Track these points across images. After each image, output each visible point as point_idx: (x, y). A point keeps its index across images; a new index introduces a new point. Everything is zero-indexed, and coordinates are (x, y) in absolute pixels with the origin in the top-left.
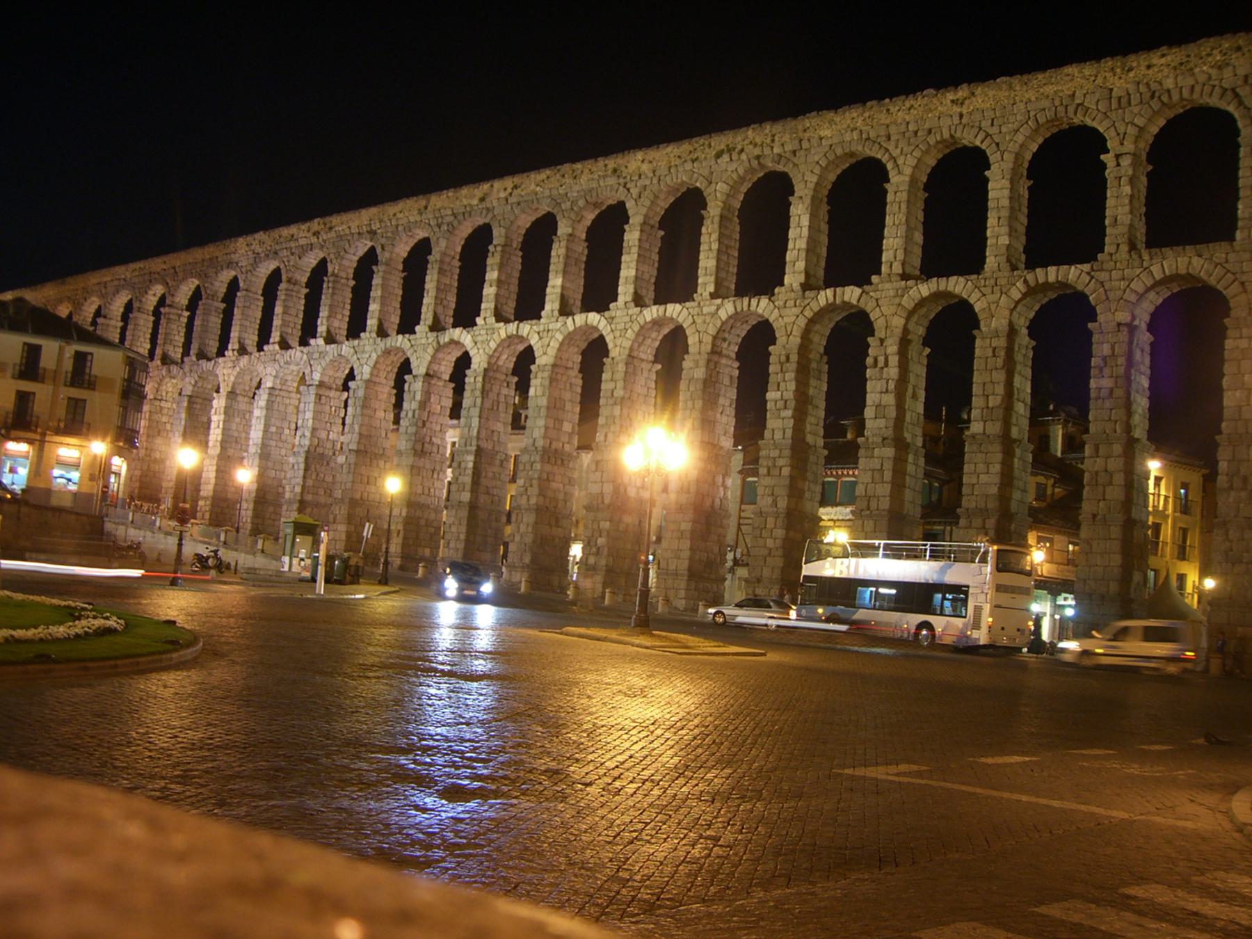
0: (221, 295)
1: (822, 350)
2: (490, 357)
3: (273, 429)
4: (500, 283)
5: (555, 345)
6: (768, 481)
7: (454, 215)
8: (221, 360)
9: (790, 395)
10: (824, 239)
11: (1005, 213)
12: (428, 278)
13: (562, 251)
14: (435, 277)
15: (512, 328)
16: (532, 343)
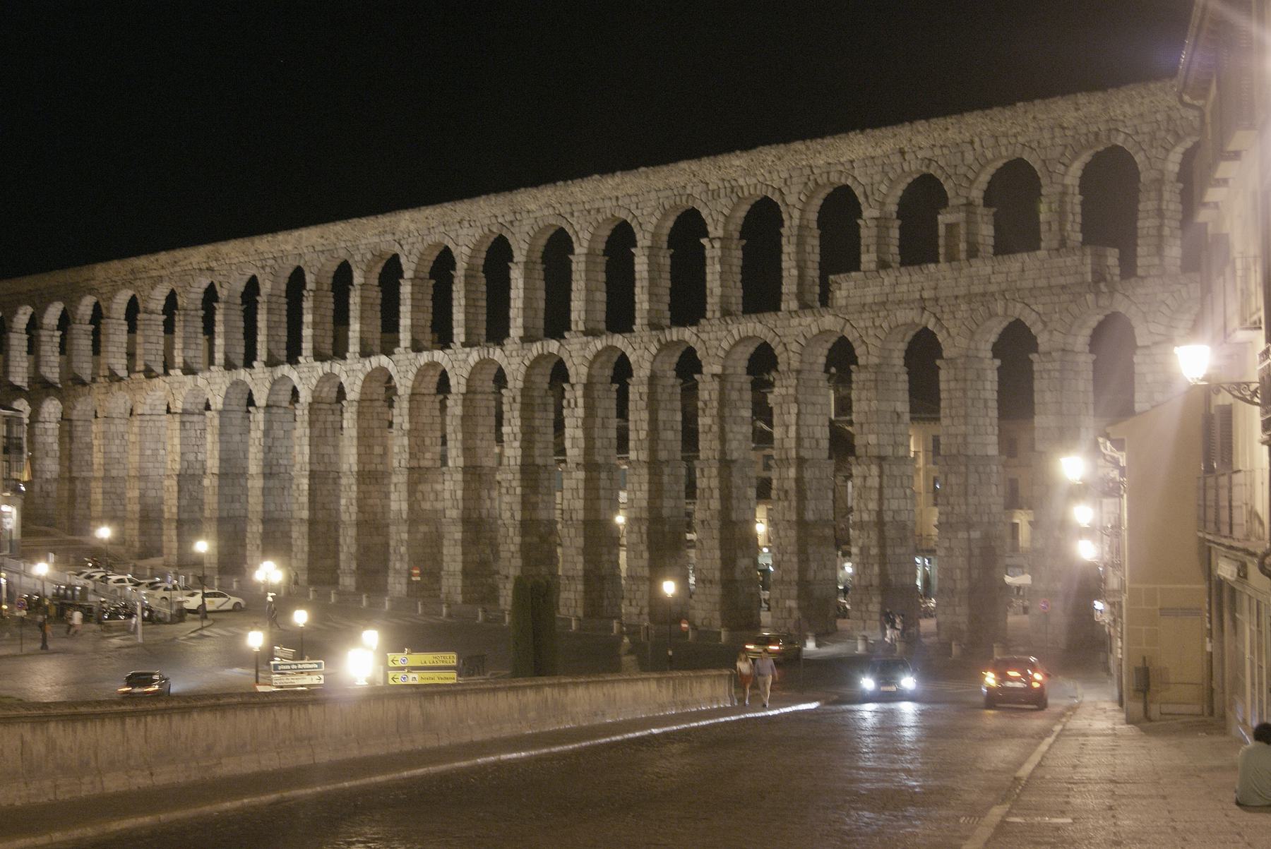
0: (88, 318)
1: (546, 386)
2: (313, 392)
3: (149, 452)
4: (315, 325)
5: (359, 383)
6: (507, 499)
7: (274, 258)
8: (94, 386)
9: (517, 430)
10: (541, 294)
11: (646, 283)
12: (259, 317)
13: (358, 300)
14: (265, 317)
15: (327, 366)
16: (342, 380)
